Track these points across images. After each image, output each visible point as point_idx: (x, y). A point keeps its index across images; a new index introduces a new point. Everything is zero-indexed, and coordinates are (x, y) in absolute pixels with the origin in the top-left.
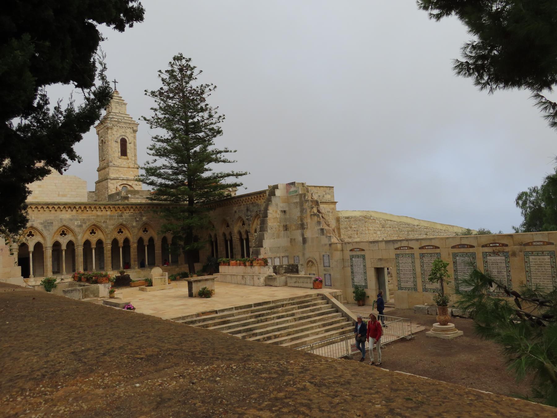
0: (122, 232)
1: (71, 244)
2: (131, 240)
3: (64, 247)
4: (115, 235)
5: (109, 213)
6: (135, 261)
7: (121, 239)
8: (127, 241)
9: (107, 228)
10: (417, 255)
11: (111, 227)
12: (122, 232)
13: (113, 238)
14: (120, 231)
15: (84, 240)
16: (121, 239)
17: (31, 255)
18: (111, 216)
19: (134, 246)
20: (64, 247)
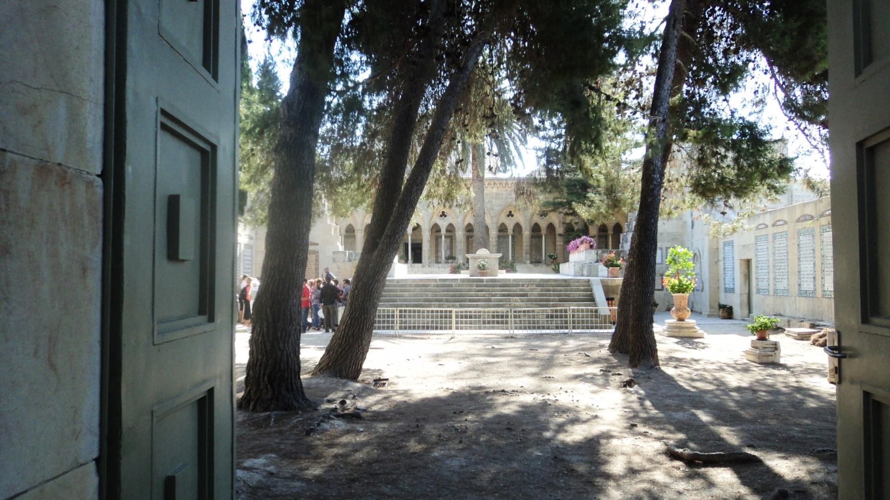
0: (512, 216)
1: (451, 229)
2: (523, 226)
3: (443, 231)
4: (504, 219)
5: (495, 190)
6: (526, 253)
7: (510, 224)
8: (518, 227)
9: (492, 209)
10: (770, 238)
11: (498, 208)
12: (512, 216)
13: (500, 222)
14: (510, 214)
15: (466, 223)
16: (510, 224)
17: (410, 238)
18: (497, 194)
19: (526, 233)
20: (443, 231)
